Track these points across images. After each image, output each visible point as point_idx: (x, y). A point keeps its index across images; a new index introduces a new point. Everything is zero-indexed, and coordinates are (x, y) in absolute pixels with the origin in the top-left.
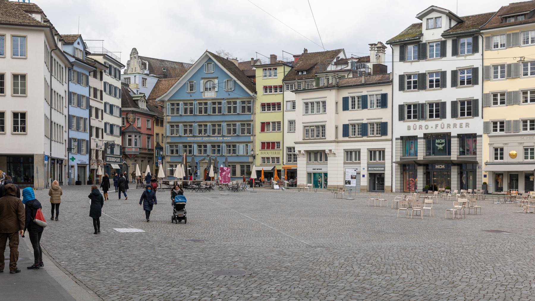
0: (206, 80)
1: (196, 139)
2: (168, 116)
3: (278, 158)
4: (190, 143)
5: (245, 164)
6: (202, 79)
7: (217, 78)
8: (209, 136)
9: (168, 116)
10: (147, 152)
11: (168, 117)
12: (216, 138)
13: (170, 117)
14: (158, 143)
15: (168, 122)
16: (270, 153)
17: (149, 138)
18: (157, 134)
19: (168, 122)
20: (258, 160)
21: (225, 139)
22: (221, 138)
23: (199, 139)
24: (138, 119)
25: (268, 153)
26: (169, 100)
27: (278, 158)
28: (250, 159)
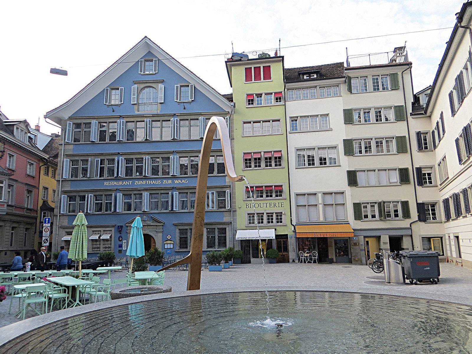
0: (143, 86)
1: (120, 183)
2: (68, 144)
3: (279, 215)
4: (110, 190)
5: (216, 227)
6: (135, 83)
7: (162, 82)
8: (146, 178)
9: (68, 144)
10: (24, 213)
11: (67, 147)
12: (159, 182)
13: (71, 147)
14: (45, 202)
15: (68, 156)
16: (266, 206)
17: (29, 192)
18: (46, 189)
19: (68, 156)
20: (241, 218)
21: (176, 182)
22: (170, 181)
23: (125, 183)
24: (11, 156)
25: (259, 205)
26: (70, 118)
27: (279, 215)
28: (226, 219)
